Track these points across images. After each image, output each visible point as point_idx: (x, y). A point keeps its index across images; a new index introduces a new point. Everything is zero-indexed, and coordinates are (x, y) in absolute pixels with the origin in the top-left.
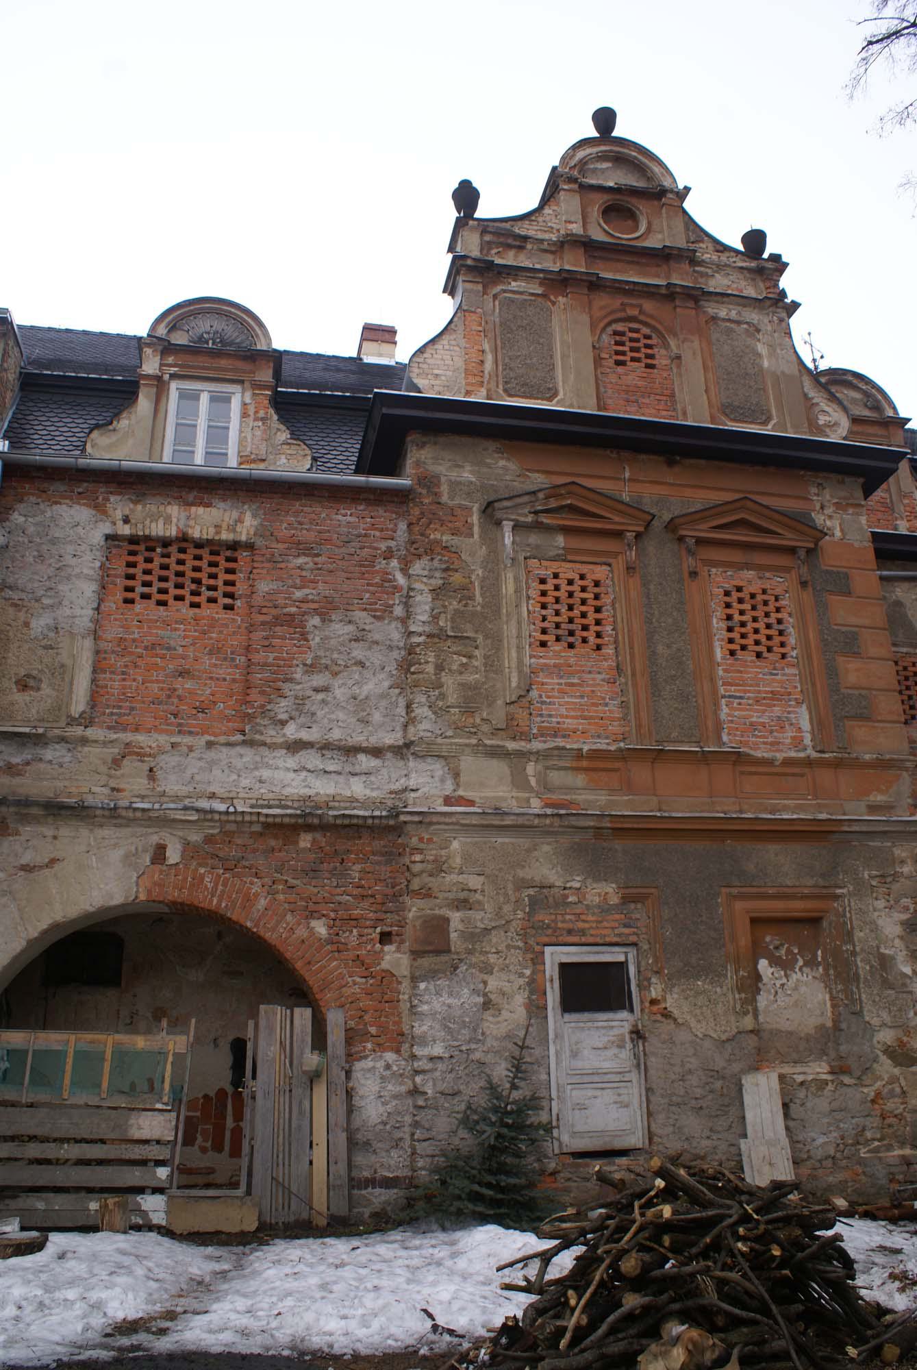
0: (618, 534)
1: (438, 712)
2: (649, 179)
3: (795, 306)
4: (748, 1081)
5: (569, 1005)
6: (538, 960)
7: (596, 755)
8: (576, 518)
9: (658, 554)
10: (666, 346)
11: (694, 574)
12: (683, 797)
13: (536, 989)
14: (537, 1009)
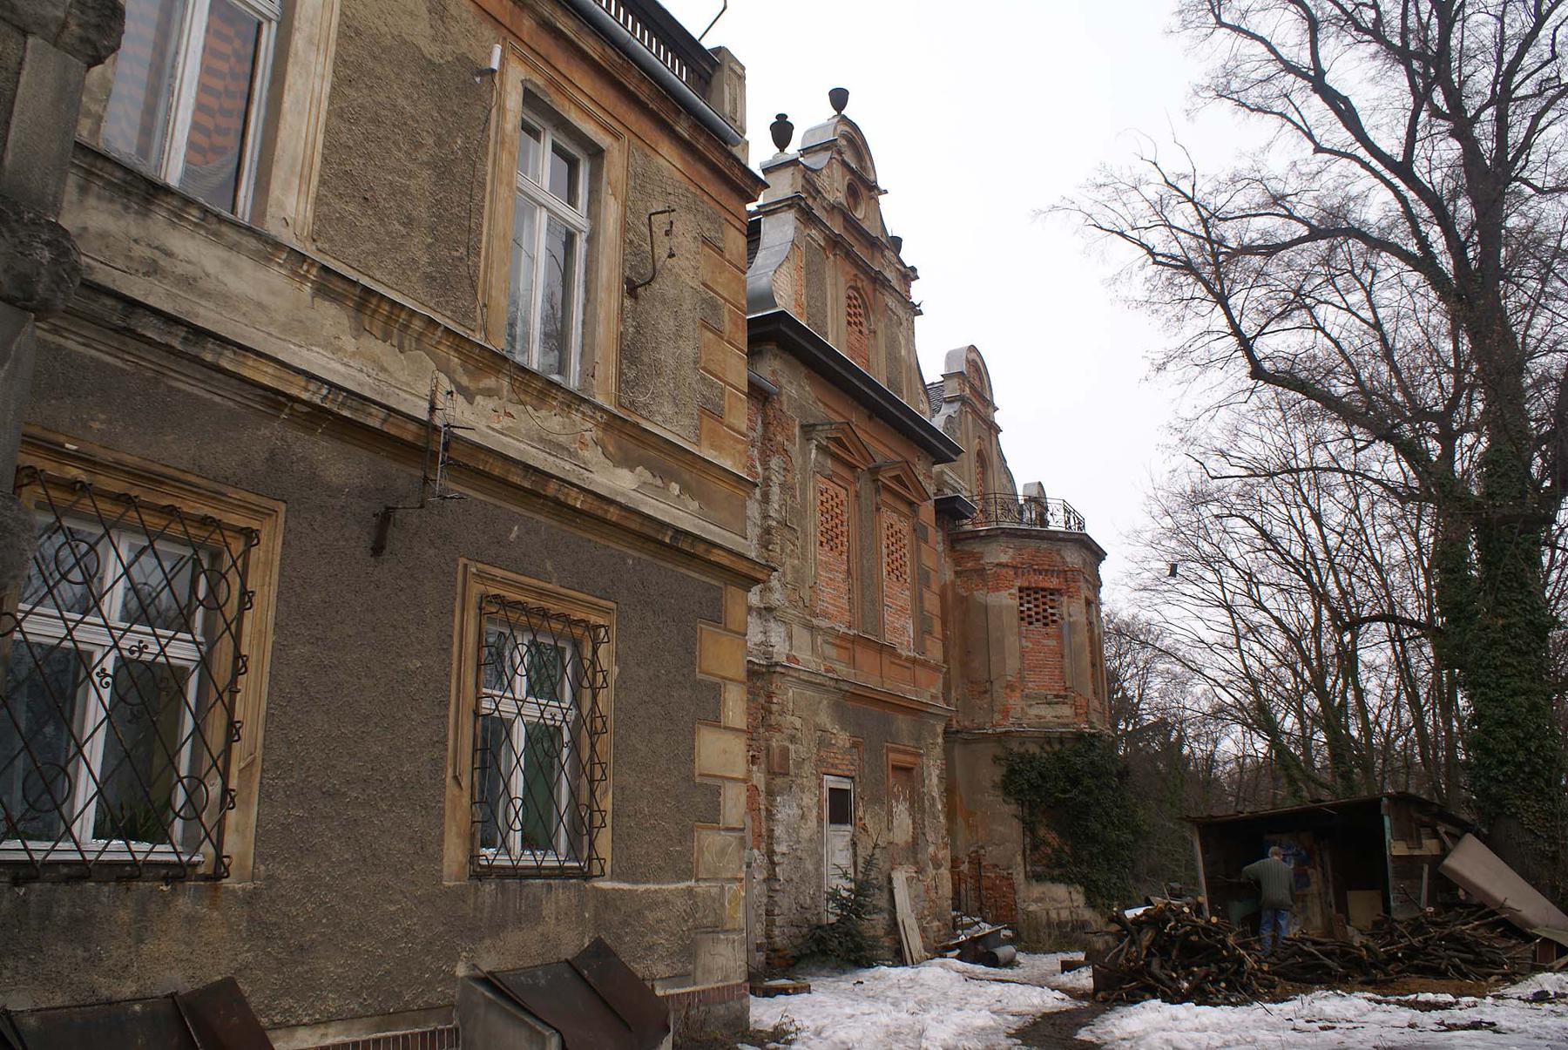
0: (852, 467)
1: (784, 585)
2: (864, 168)
3: (920, 313)
4: (894, 875)
5: (833, 821)
6: (820, 786)
7: (844, 637)
8: (841, 452)
9: (864, 486)
10: (868, 319)
11: (878, 509)
12: (869, 674)
13: (821, 808)
14: (820, 820)
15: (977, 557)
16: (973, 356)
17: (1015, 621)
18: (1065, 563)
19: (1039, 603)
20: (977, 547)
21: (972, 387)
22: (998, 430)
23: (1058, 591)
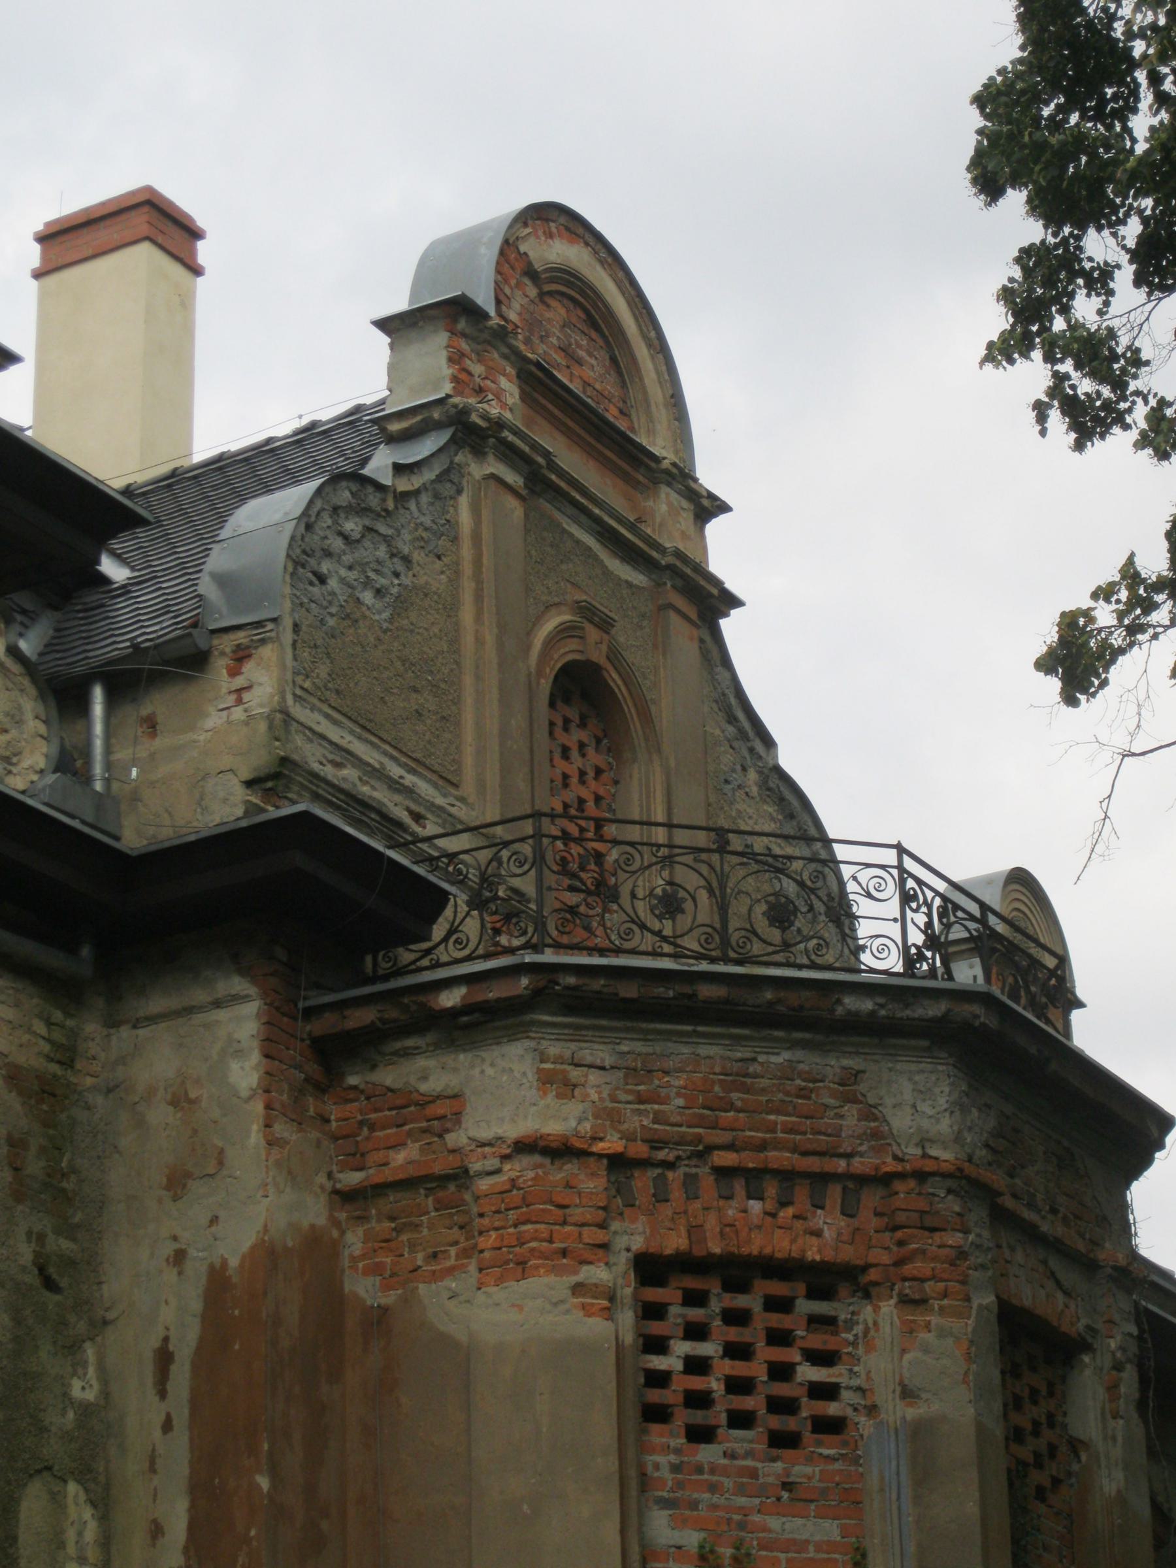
15: (438, 1115)
16: (560, 252)
17: (602, 1425)
18: (879, 1137)
19: (754, 1335)
20: (430, 1072)
21: (538, 382)
22: (713, 601)
23: (826, 1279)
